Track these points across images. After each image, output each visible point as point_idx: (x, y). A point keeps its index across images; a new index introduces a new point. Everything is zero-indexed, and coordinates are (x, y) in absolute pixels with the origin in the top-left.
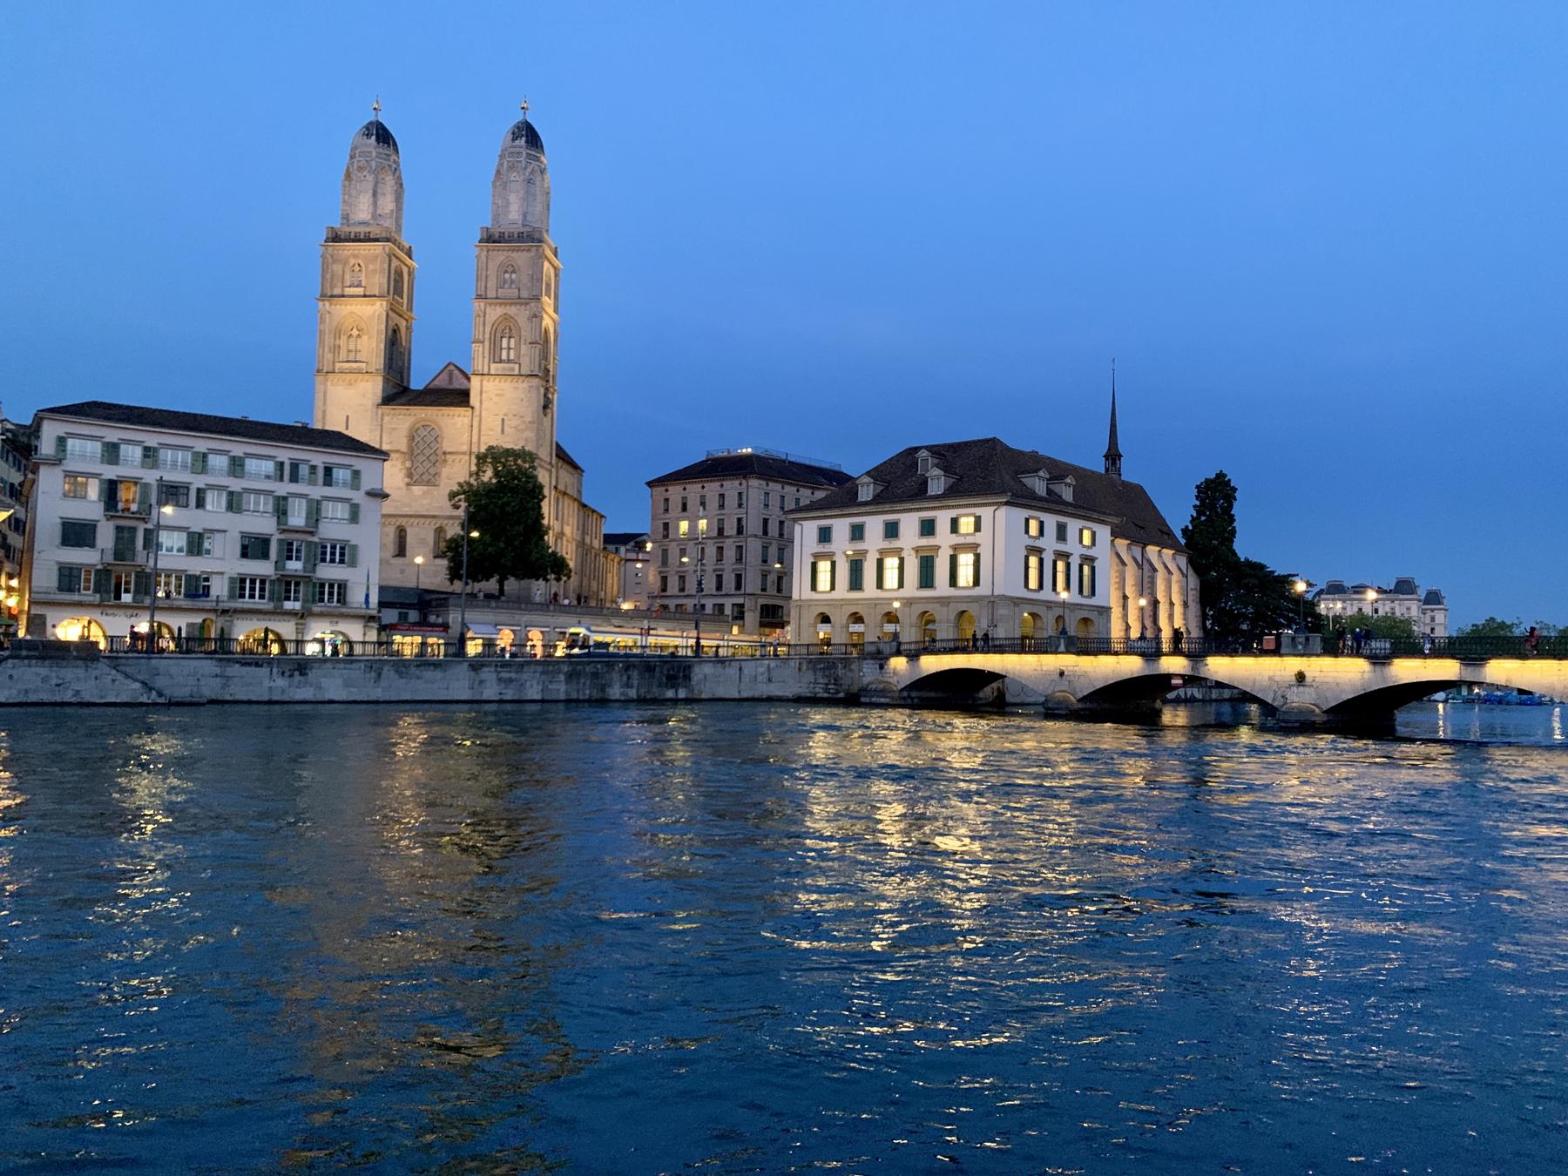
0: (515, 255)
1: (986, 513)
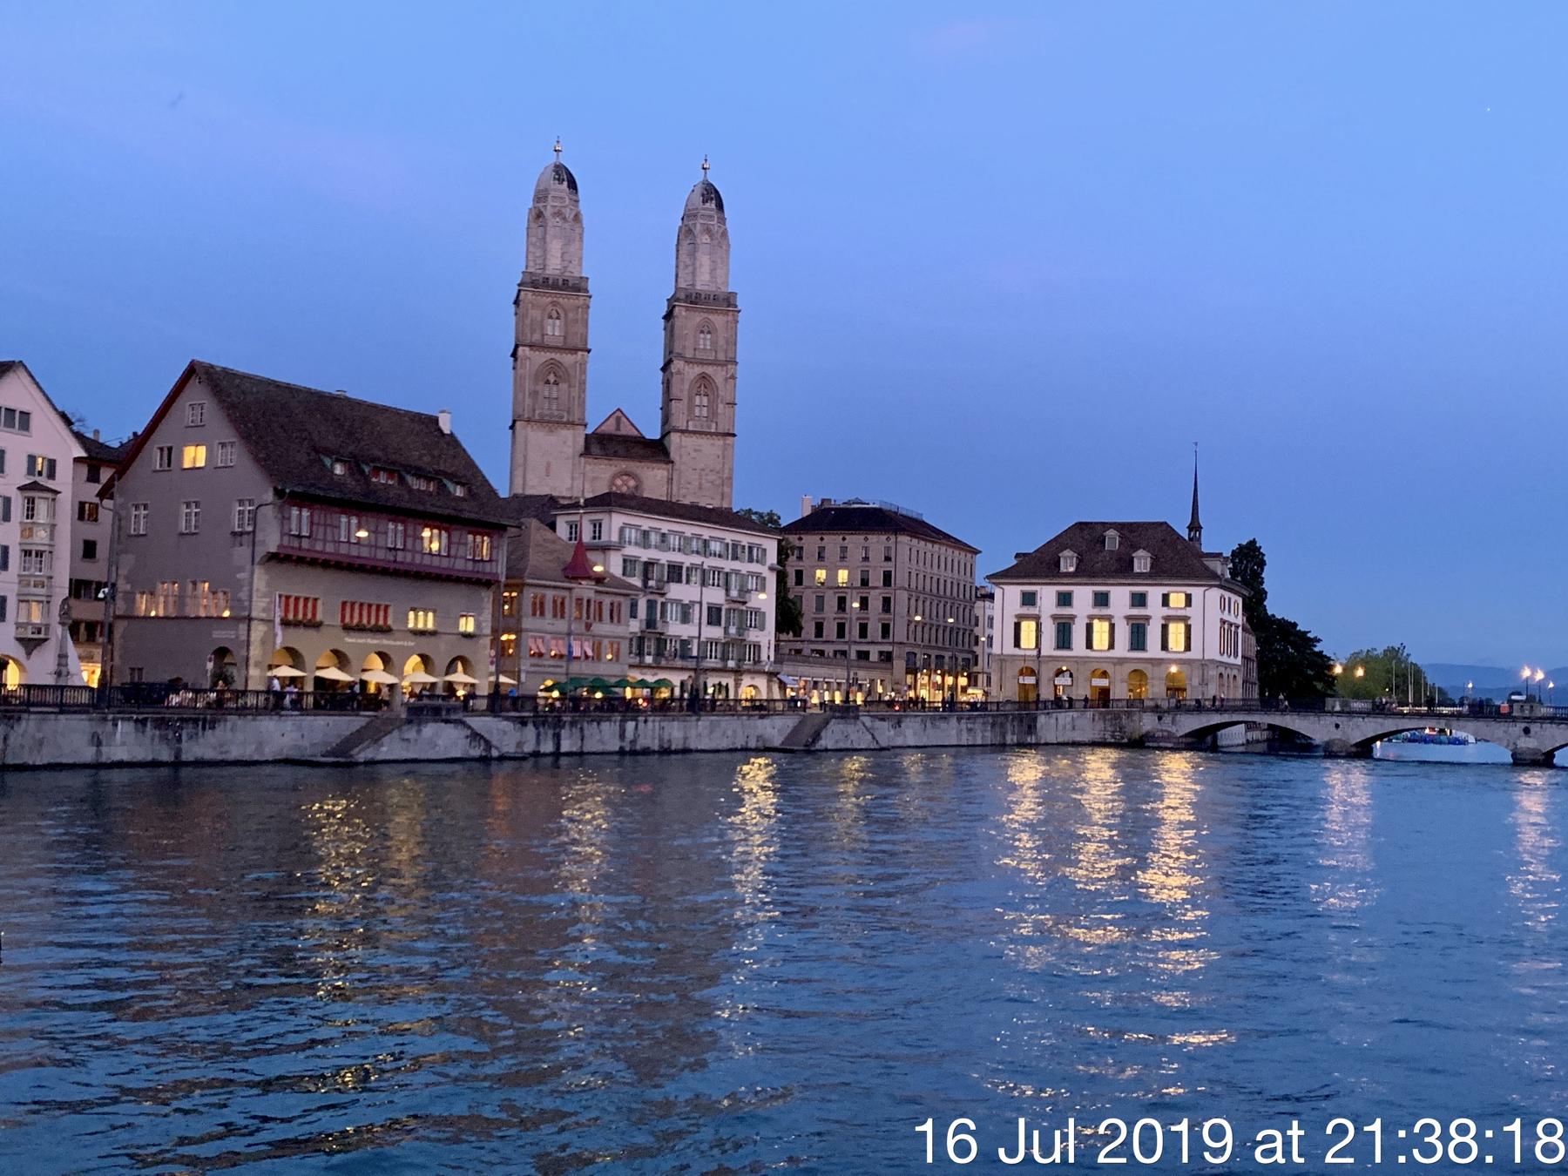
0: (711, 317)
1: (1197, 592)
